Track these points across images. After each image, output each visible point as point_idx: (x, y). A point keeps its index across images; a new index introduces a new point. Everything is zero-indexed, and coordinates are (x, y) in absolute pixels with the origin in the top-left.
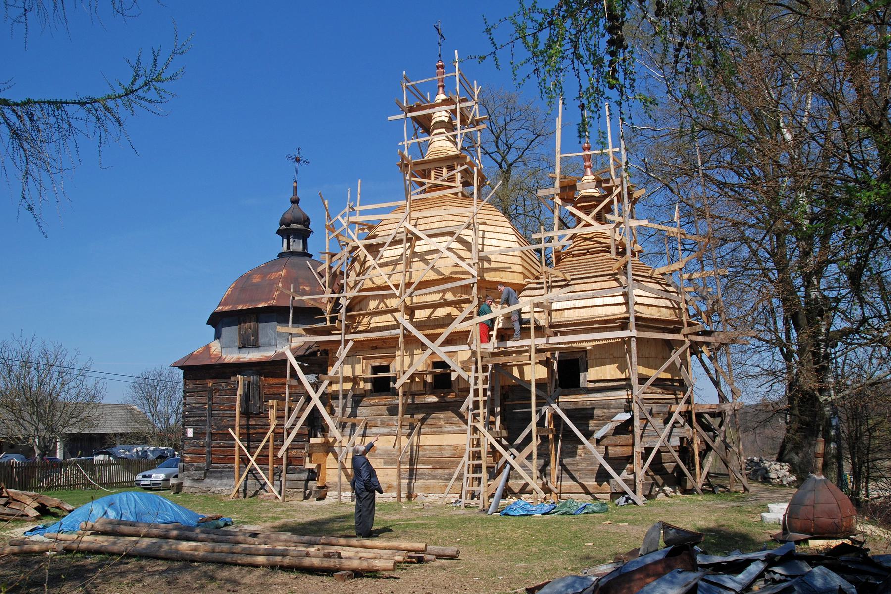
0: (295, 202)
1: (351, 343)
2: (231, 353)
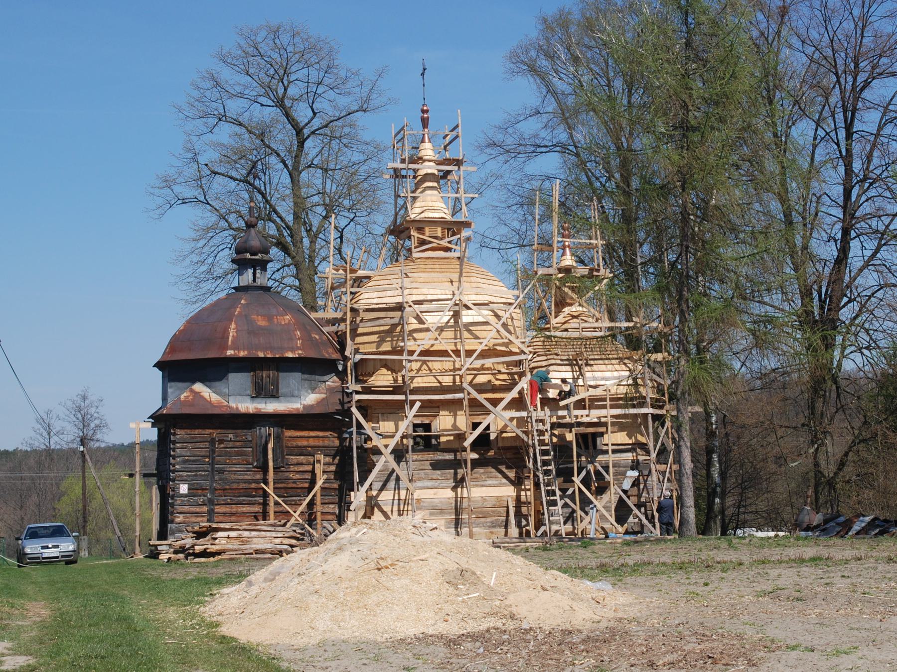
1: (418, 404)
2: (242, 402)
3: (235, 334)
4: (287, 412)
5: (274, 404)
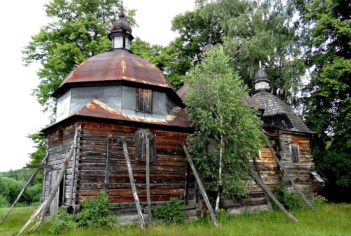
2: (130, 114)
3: (126, 68)
4: (160, 124)
5: (151, 118)
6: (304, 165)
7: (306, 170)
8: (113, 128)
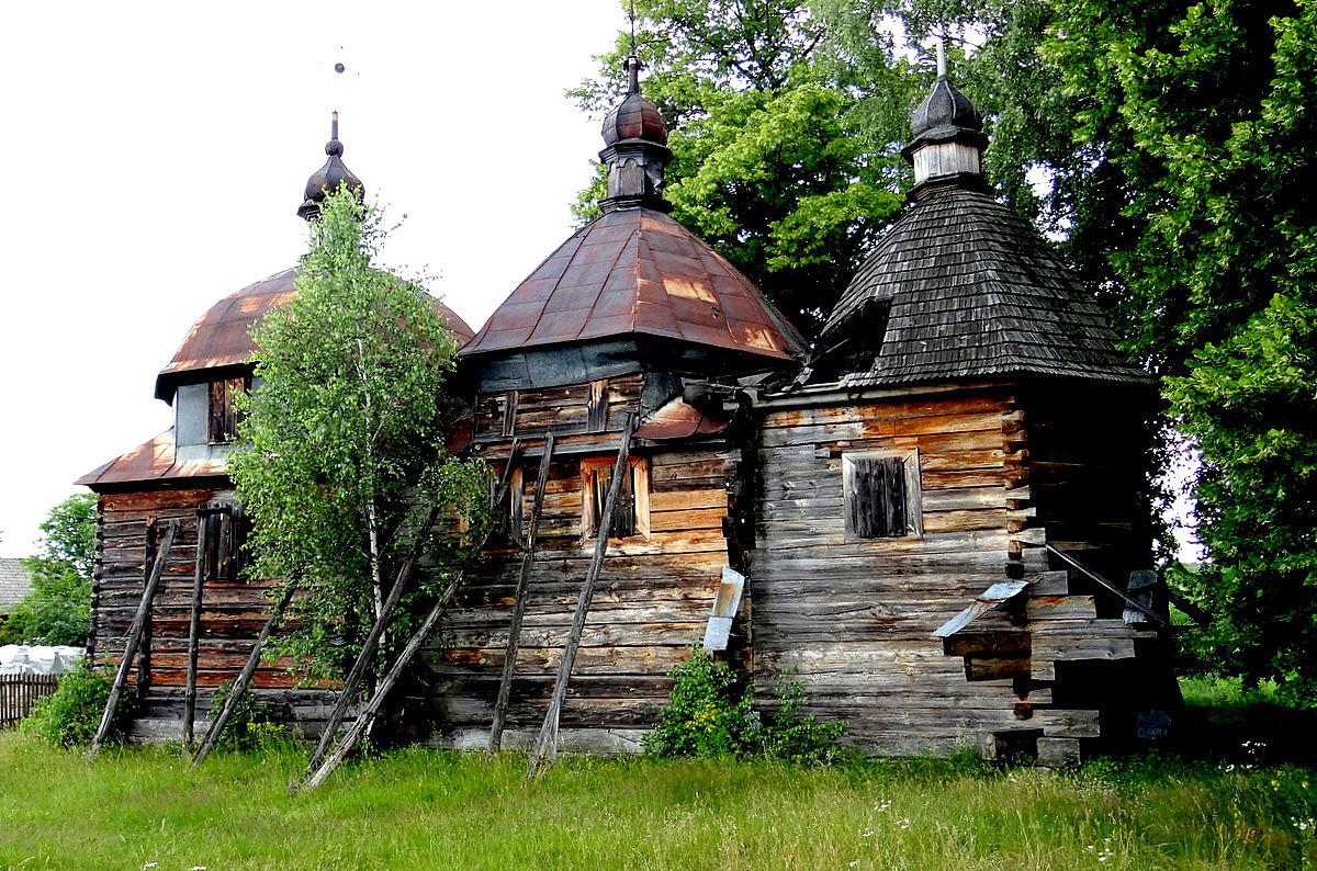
0: (335, 151)
2: (193, 457)
6: (951, 550)
7: (959, 572)
8: (158, 501)
